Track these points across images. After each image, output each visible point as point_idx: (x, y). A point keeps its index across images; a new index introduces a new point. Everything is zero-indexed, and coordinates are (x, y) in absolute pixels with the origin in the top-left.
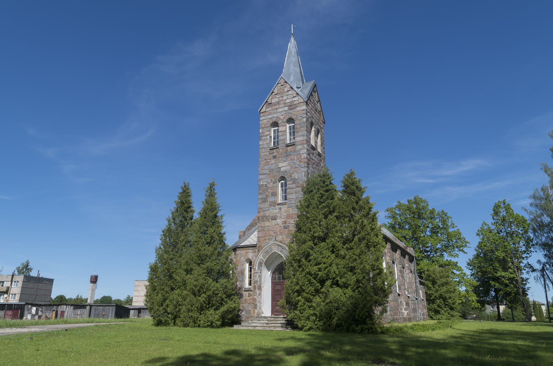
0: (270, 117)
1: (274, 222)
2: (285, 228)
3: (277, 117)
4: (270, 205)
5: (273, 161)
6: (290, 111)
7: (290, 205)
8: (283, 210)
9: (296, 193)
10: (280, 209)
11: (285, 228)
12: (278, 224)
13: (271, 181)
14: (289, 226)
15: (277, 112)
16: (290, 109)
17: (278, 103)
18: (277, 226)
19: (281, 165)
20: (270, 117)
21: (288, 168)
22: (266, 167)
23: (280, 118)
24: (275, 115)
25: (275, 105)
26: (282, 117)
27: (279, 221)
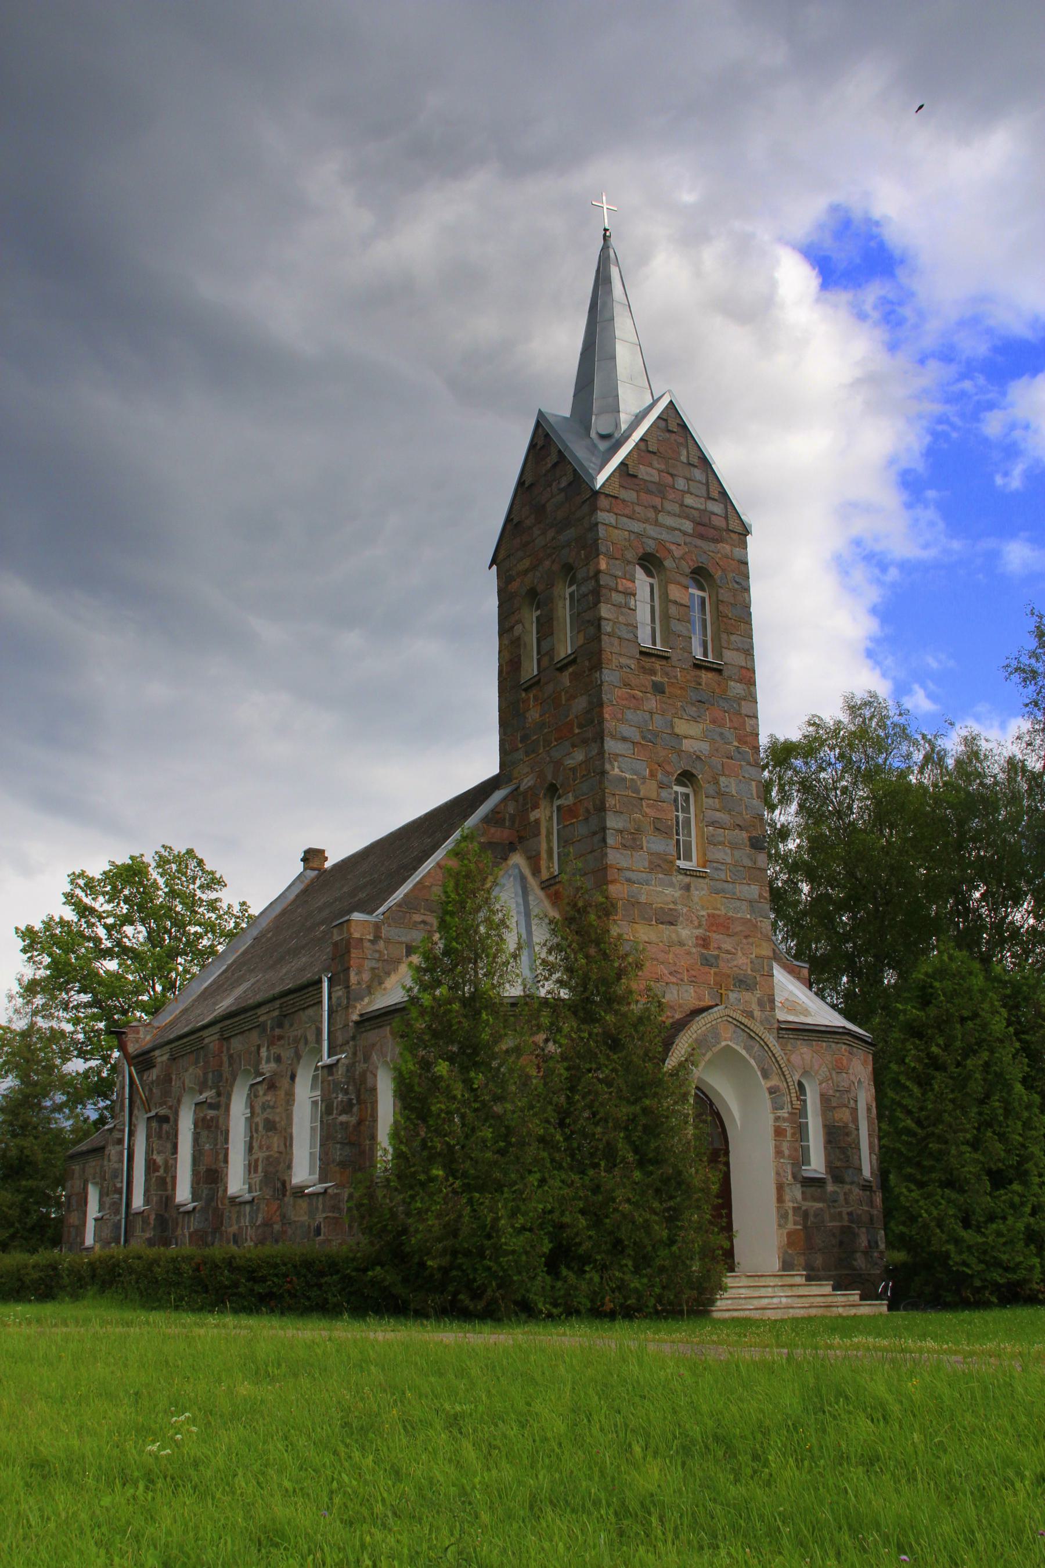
0: (636, 527)
1: (666, 930)
2: (706, 962)
3: (660, 543)
4: (653, 868)
5: (652, 703)
6: (699, 542)
7: (720, 885)
8: (695, 894)
9: (734, 846)
10: (687, 888)
11: (706, 962)
12: (681, 944)
13: (652, 775)
14: (717, 957)
15: (656, 523)
16: (702, 537)
17: (661, 490)
18: (677, 949)
19: (682, 727)
20: (636, 527)
21: (704, 747)
22: (629, 715)
23: (669, 551)
24: (651, 531)
25: (649, 492)
26: (677, 552)
27: (685, 932)
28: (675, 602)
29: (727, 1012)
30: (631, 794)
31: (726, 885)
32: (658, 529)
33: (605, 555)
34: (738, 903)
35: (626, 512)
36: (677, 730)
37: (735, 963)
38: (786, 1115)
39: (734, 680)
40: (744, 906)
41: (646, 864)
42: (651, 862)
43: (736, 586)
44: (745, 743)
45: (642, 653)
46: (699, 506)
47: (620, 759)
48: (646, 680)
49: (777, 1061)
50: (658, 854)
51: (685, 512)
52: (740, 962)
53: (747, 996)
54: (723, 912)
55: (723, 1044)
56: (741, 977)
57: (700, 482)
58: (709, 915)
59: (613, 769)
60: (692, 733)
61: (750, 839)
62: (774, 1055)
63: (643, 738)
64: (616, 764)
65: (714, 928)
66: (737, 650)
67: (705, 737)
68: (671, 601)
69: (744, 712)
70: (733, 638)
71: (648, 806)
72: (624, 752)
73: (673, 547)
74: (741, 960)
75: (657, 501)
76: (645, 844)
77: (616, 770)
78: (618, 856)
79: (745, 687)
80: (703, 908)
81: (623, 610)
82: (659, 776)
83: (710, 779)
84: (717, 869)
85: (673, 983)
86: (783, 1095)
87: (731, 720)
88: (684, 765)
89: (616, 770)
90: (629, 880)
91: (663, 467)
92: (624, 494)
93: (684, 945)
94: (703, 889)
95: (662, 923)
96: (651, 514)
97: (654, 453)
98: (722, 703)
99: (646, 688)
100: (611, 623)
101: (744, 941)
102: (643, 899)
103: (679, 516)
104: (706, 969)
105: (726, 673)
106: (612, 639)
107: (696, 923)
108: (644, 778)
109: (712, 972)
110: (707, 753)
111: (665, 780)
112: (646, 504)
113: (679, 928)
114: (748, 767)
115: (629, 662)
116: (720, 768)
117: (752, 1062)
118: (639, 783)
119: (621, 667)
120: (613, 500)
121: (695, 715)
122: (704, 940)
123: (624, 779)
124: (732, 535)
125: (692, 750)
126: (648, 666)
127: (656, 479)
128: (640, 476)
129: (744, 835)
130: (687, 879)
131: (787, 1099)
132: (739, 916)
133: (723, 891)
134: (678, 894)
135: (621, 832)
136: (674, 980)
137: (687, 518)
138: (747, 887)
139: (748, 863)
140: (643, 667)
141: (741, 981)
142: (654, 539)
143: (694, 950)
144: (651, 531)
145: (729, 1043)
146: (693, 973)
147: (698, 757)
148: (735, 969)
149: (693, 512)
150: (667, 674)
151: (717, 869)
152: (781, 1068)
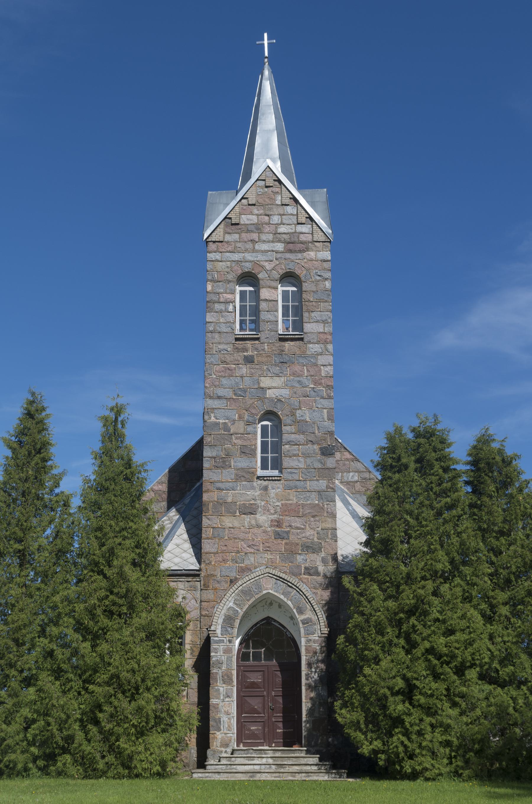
0: (236, 257)
1: (247, 519)
2: (278, 536)
3: (255, 263)
4: (238, 478)
5: (244, 370)
6: (288, 255)
7: (291, 484)
8: (272, 492)
9: (306, 456)
10: (266, 488)
11: (278, 536)
12: (259, 526)
13: (241, 418)
14: (288, 533)
15: (254, 251)
16: (291, 251)
17: (258, 228)
18: (256, 530)
19: (265, 382)
20: (236, 257)
21: (285, 392)
22: (224, 381)
23: (263, 267)
24: (249, 257)
25: (248, 231)
26: (268, 266)
27: (262, 518)
28: (266, 300)
29: (267, 570)
30: (223, 432)
31: (298, 483)
32: (254, 254)
33: (211, 281)
34: (308, 494)
35: (230, 249)
36: (262, 385)
37: (303, 535)
38: (317, 638)
39: (313, 343)
40: (314, 495)
41: (233, 476)
42: (237, 475)
43: (318, 278)
44: (320, 384)
45: (237, 339)
46: (290, 231)
47: (216, 411)
48: (239, 356)
49: (310, 602)
50: (242, 469)
51: (277, 237)
52: (308, 534)
53: (313, 556)
54: (295, 501)
55: (265, 592)
56: (308, 544)
57: (292, 215)
58: (282, 505)
59: (210, 418)
60: (274, 385)
61: (321, 449)
62: (307, 597)
63: (235, 394)
64: (212, 415)
65: (287, 513)
66: (317, 322)
67: (286, 385)
68: (262, 300)
69: (320, 363)
70: (313, 314)
71: (236, 438)
72: (219, 406)
73: (266, 264)
74: (309, 533)
75: (255, 236)
76: (232, 464)
77: (213, 418)
78: (211, 474)
79: (322, 346)
80: (278, 501)
81: (223, 314)
82: (246, 417)
83: (289, 413)
84: (291, 473)
85: (251, 553)
86: (315, 624)
87: (308, 370)
88: (268, 407)
89: (213, 418)
90: (219, 489)
91: (261, 212)
92: (228, 238)
93: (261, 527)
94: (278, 488)
95: (244, 514)
96: (250, 246)
97: (254, 205)
98: (301, 360)
99: (239, 361)
100: (213, 324)
101: (312, 519)
102: (230, 500)
103: (273, 242)
104: (279, 541)
105: (306, 340)
106: (214, 334)
107: (272, 511)
108: (234, 421)
109: (283, 543)
110: (287, 397)
111: (251, 419)
112: (246, 240)
113: (258, 516)
114: (322, 400)
115: (225, 347)
116: (297, 404)
117: (289, 603)
118: (229, 424)
119: (220, 351)
120: (220, 244)
121: (278, 372)
122: (278, 522)
123: (218, 424)
124: (316, 244)
125: (274, 396)
126: (240, 347)
127: (255, 221)
128: (242, 222)
129: (316, 447)
130: (266, 483)
131: (317, 627)
132: (309, 502)
133: (296, 487)
134: (258, 493)
135: (215, 458)
136: (252, 550)
137: (280, 241)
138: (316, 482)
139: (318, 465)
140: (237, 348)
141: (307, 547)
142: (251, 262)
143: (269, 529)
144: (249, 257)
145: (270, 591)
146: (267, 544)
147: (279, 400)
148: (303, 539)
149: (284, 236)
150: (256, 349)
151: (291, 473)
152: (312, 606)
